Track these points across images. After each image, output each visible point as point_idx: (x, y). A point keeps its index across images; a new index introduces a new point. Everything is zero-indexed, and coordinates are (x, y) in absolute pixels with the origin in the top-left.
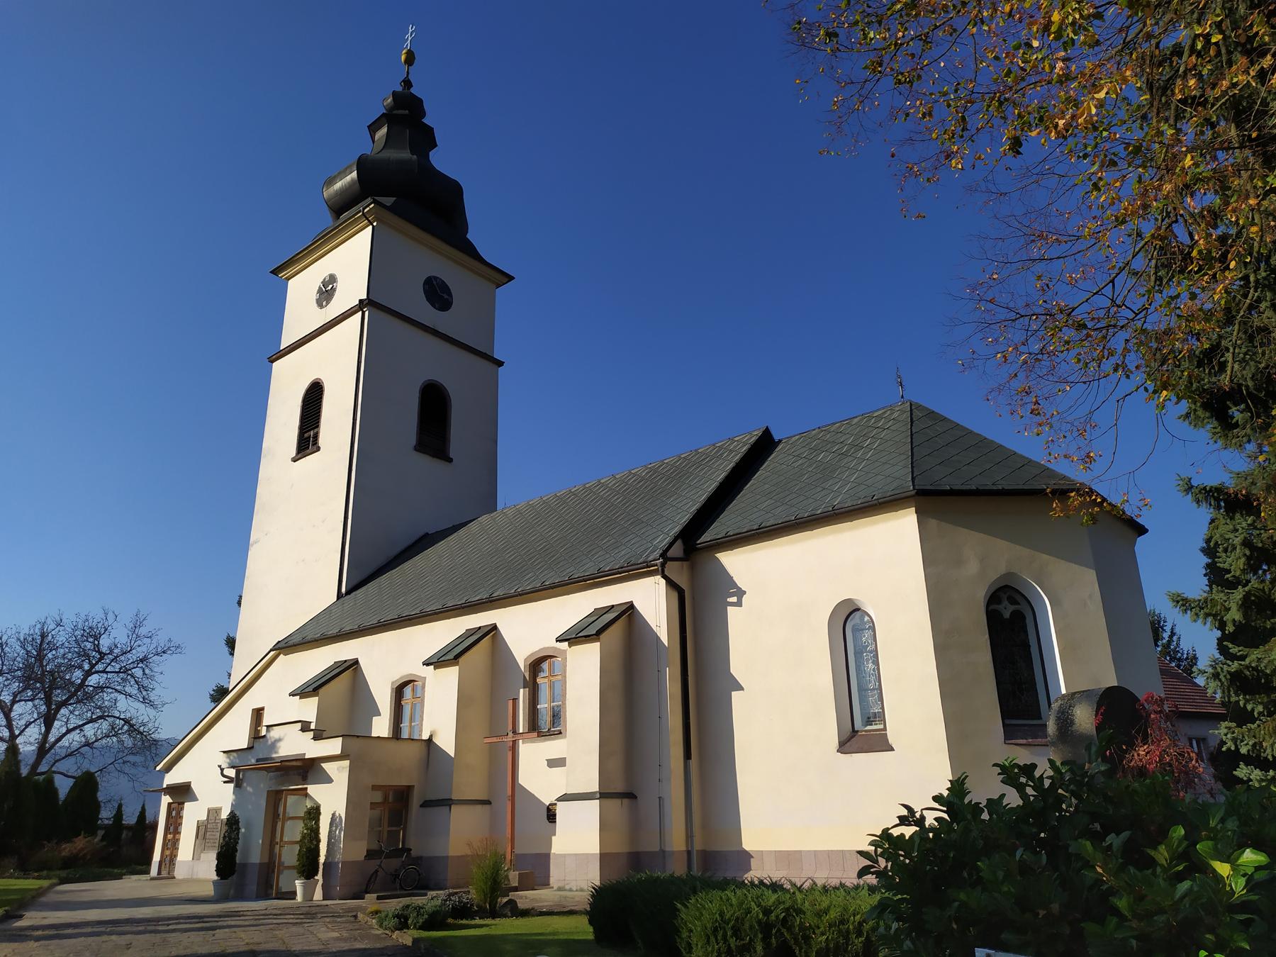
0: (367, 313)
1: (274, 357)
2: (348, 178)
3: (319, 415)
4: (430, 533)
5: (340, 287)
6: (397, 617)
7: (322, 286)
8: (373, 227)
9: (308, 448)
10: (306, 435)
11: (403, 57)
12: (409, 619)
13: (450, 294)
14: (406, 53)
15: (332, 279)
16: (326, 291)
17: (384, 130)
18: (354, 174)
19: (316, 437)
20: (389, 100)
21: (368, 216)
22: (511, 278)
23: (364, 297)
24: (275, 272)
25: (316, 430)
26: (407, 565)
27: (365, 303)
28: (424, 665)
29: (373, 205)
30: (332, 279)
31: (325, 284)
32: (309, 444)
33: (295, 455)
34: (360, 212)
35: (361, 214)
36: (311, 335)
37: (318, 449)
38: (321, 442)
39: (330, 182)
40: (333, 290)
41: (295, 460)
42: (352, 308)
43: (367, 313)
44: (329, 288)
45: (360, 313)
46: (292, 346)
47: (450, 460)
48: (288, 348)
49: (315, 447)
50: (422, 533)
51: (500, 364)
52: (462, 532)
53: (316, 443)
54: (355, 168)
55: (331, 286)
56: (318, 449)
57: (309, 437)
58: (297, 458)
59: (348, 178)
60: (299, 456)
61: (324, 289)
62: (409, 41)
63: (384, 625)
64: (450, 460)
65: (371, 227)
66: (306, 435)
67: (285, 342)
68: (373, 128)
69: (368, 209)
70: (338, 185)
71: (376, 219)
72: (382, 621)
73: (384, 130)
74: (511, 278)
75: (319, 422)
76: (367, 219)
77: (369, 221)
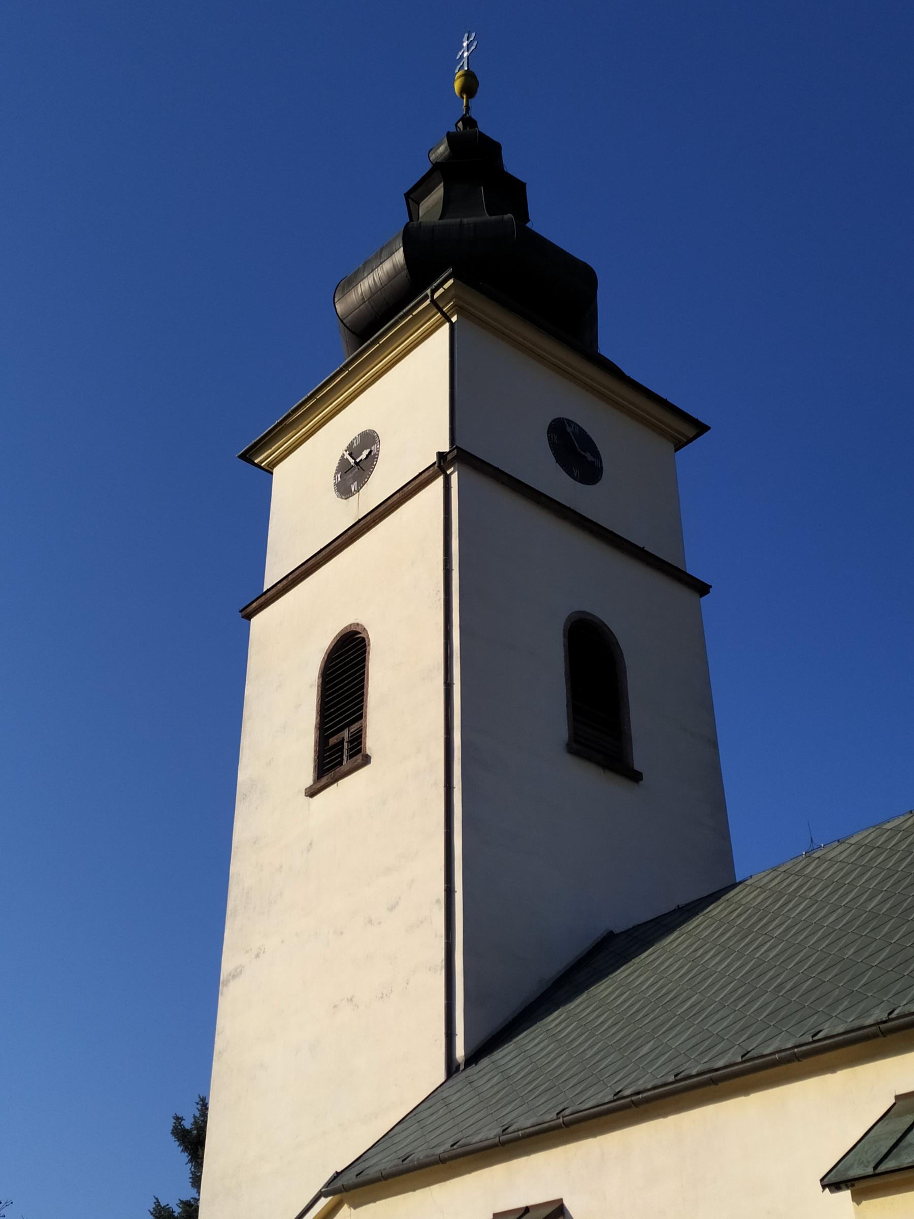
0: (454, 479)
1: (254, 605)
2: (387, 266)
3: (363, 694)
4: (617, 931)
5: (386, 450)
6: (672, 1078)
7: (347, 456)
8: (452, 326)
9: (341, 763)
10: (333, 741)
11: (457, 85)
12: (714, 1082)
13: (597, 454)
14: (463, 75)
15: (369, 439)
16: (357, 464)
17: (439, 193)
18: (399, 256)
19: (358, 740)
20: (442, 149)
21: (441, 306)
22: (702, 429)
23: (446, 448)
24: (247, 456)
25: (354, 728)
26: (602, 990)
27: (449, 457)
28: (824, 1187)
29: (451, 281)
30: (369, 439)
31: (352, 451)
32: (342, 756)
33: (311, 782)
34: (426, 297)
35: (428, 302)
36: (331, 547)
37: (367, 760)
38: (372, 743)
39: (350, 282)
40: (372, 458)
41: (312, 793)
42: (420, 474)
43: (454, 479)
44: (363, 456)
45: (440, 481)
46: (291, 577)
47: (635, 777)
48: (285, 582)
49: (359, 757)
50: (599, 933)
51: (702, 589)
52: (715, 910)
53: (360, 751)
54: (399, 243)
55: (366, 452)
56: (367, 760)
57: (342, 742)
58: (319, 785)
59: (387, 266)
60: (324, 780)
61: (352, 461)
62: (465, 60)
63: (635, 1104)
64: (635, 777)
65: (447, 325)
66: (333, 741)
67: (273, 575)
68: (414, 196)
69: (441, 291)
70: (366, 285)
71: (458, 309)
72: (627, 1092)
73: (439, 193)
74: (702, 429)
75: (362, 708)
76: (440, 310)
77: (443, 314)
